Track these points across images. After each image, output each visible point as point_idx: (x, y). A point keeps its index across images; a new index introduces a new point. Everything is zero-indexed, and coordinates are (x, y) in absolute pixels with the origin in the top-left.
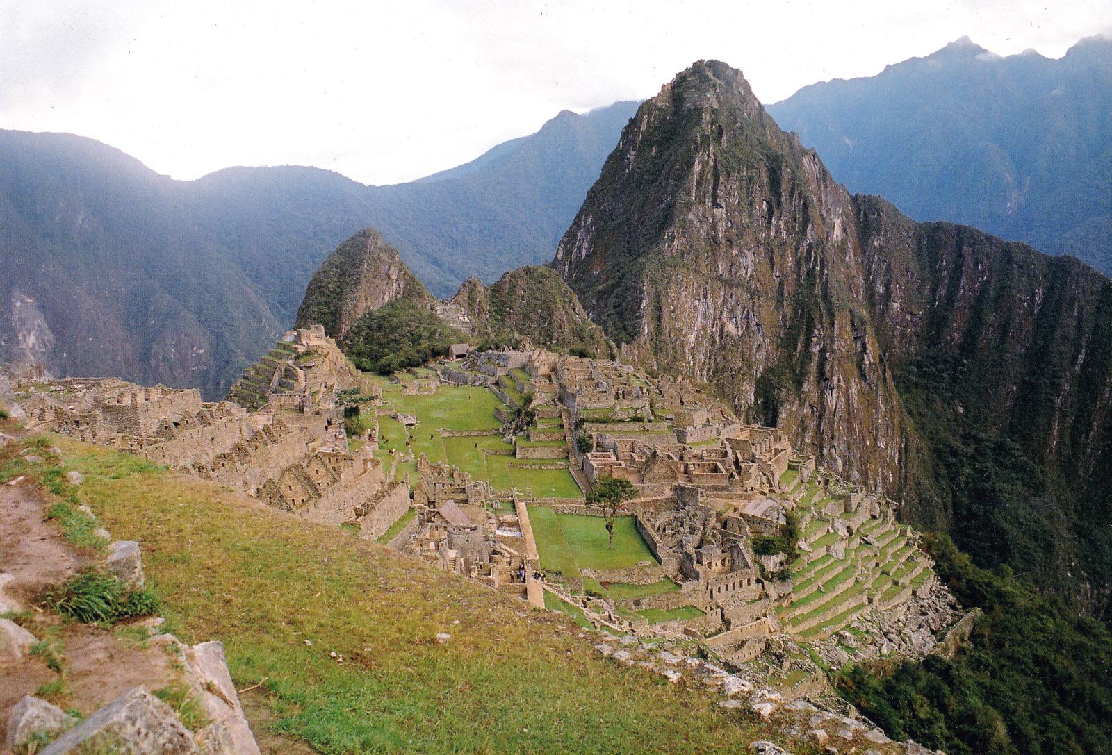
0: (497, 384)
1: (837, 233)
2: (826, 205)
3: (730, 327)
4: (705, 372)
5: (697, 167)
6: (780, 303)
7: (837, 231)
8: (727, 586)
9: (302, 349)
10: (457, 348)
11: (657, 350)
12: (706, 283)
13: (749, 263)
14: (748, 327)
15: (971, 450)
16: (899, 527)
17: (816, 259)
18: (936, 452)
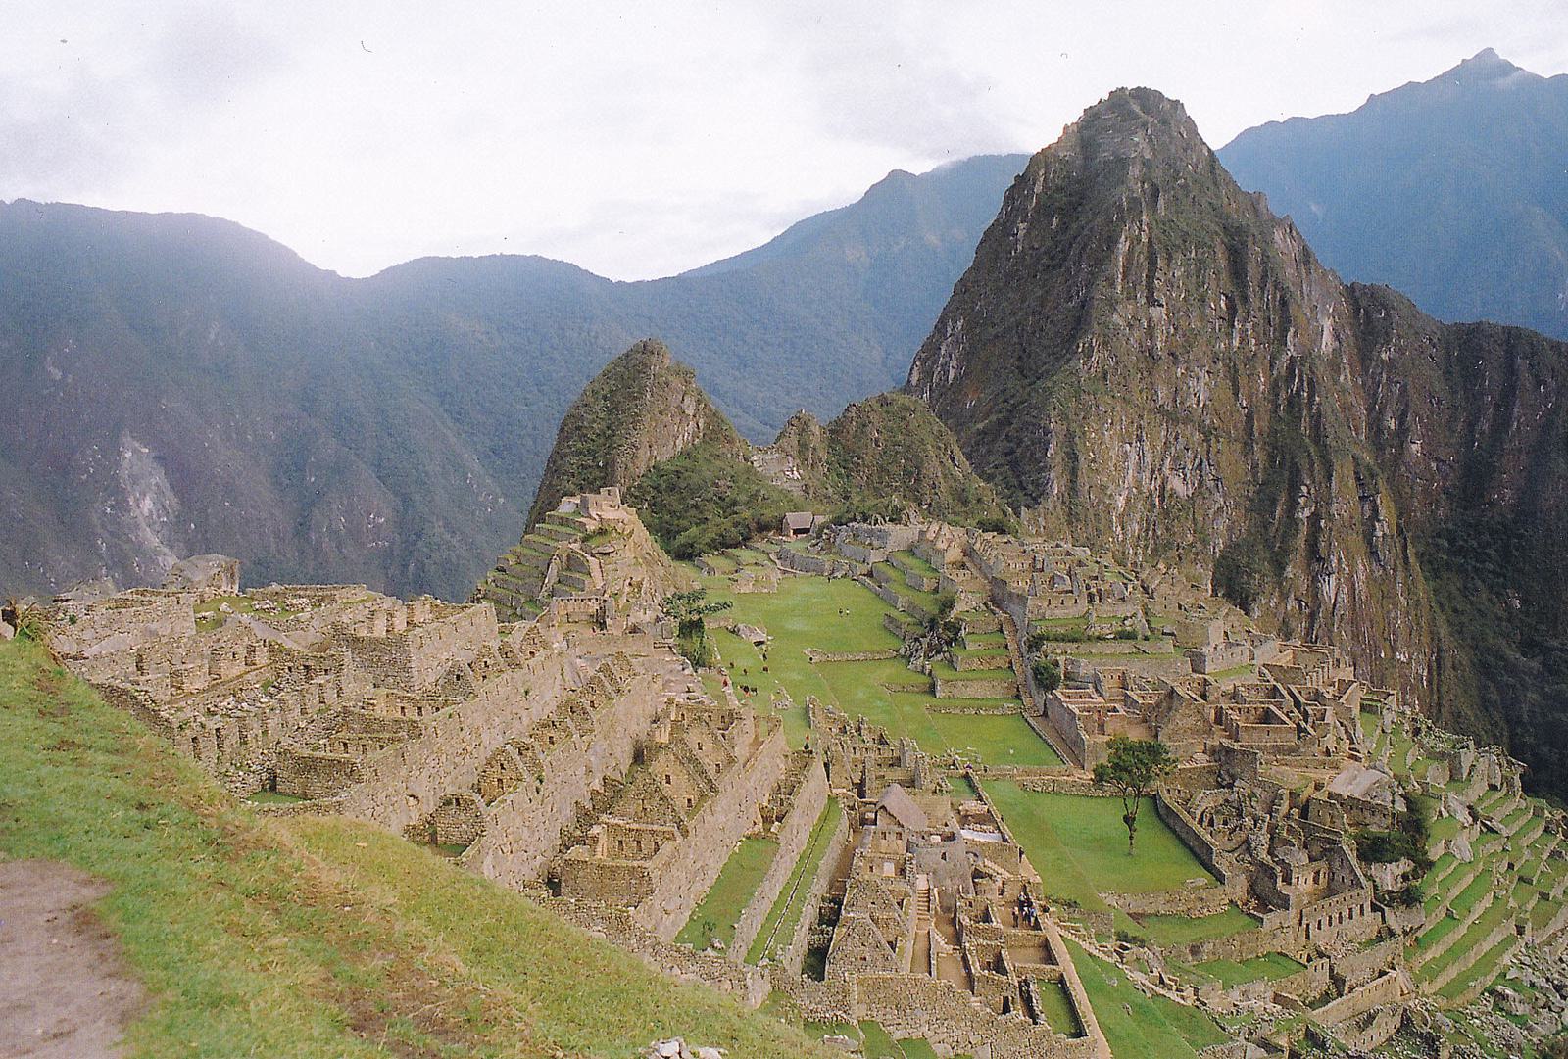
0: (870, 574)
1: (1327, 342)
2: (1310, 299)
3: (1176, 484)
4: (1140, 550)
5: (1123, 246)
6: (1248, 446)
7: (1327, 338)
8: (1330, 917)
9: (592, 526)
10: (793, 519)
11: (1072, 518)
12: (1141, 417)
13: (1202, 387)
14: (1201, 483)
15: (1535, 664)
16: (1532, 802)
17: (1301, 380)
18: (1484, 669)
